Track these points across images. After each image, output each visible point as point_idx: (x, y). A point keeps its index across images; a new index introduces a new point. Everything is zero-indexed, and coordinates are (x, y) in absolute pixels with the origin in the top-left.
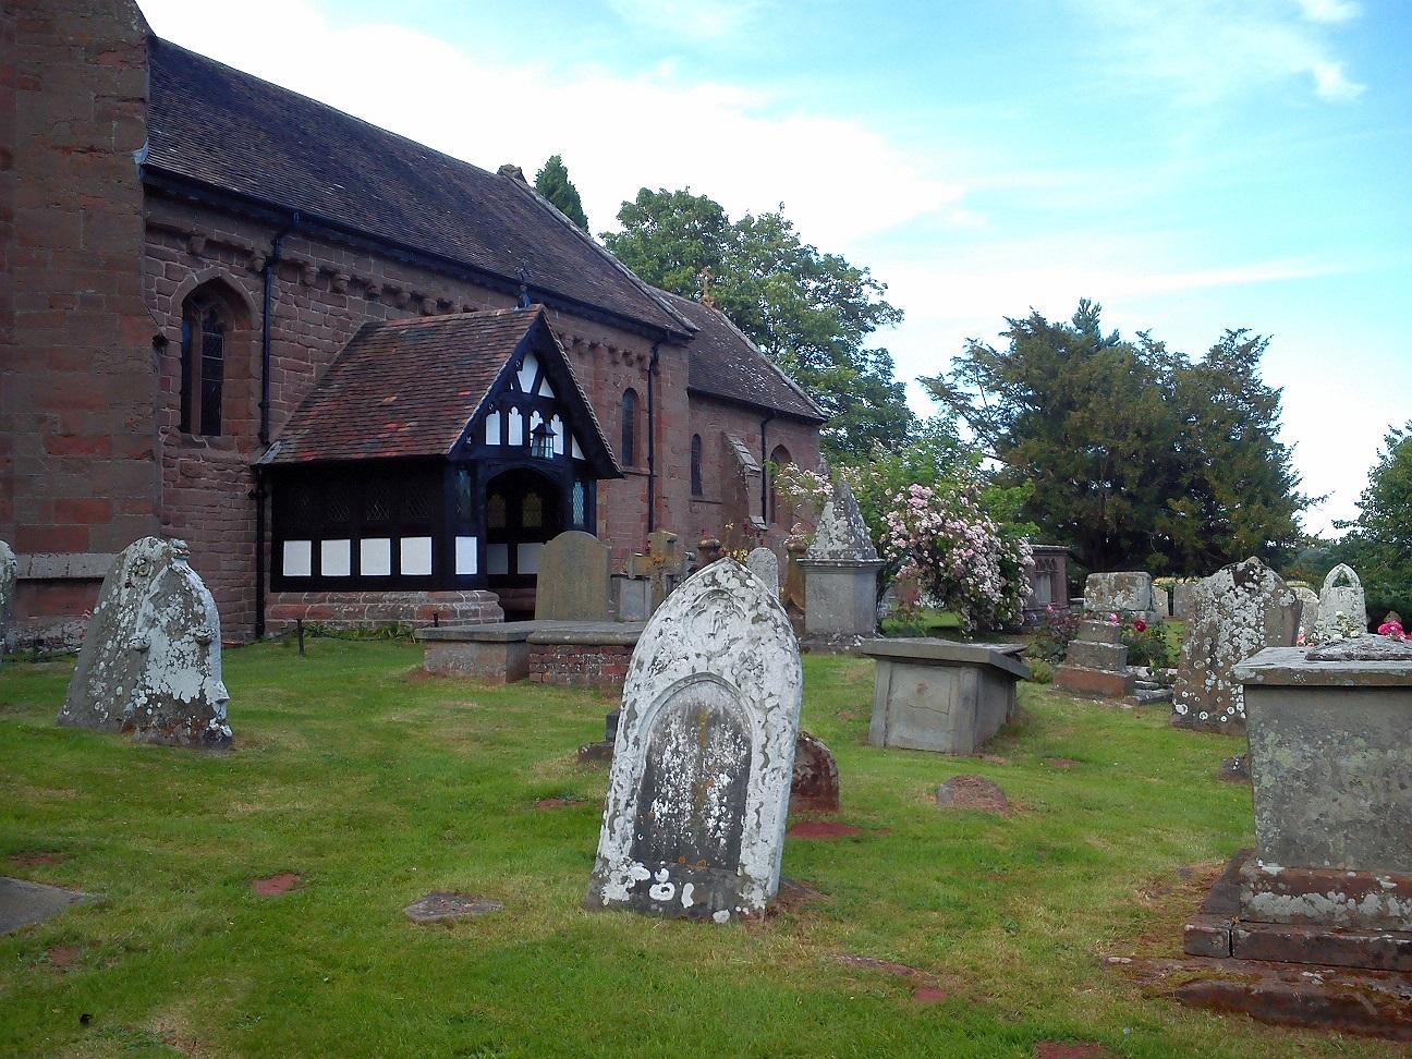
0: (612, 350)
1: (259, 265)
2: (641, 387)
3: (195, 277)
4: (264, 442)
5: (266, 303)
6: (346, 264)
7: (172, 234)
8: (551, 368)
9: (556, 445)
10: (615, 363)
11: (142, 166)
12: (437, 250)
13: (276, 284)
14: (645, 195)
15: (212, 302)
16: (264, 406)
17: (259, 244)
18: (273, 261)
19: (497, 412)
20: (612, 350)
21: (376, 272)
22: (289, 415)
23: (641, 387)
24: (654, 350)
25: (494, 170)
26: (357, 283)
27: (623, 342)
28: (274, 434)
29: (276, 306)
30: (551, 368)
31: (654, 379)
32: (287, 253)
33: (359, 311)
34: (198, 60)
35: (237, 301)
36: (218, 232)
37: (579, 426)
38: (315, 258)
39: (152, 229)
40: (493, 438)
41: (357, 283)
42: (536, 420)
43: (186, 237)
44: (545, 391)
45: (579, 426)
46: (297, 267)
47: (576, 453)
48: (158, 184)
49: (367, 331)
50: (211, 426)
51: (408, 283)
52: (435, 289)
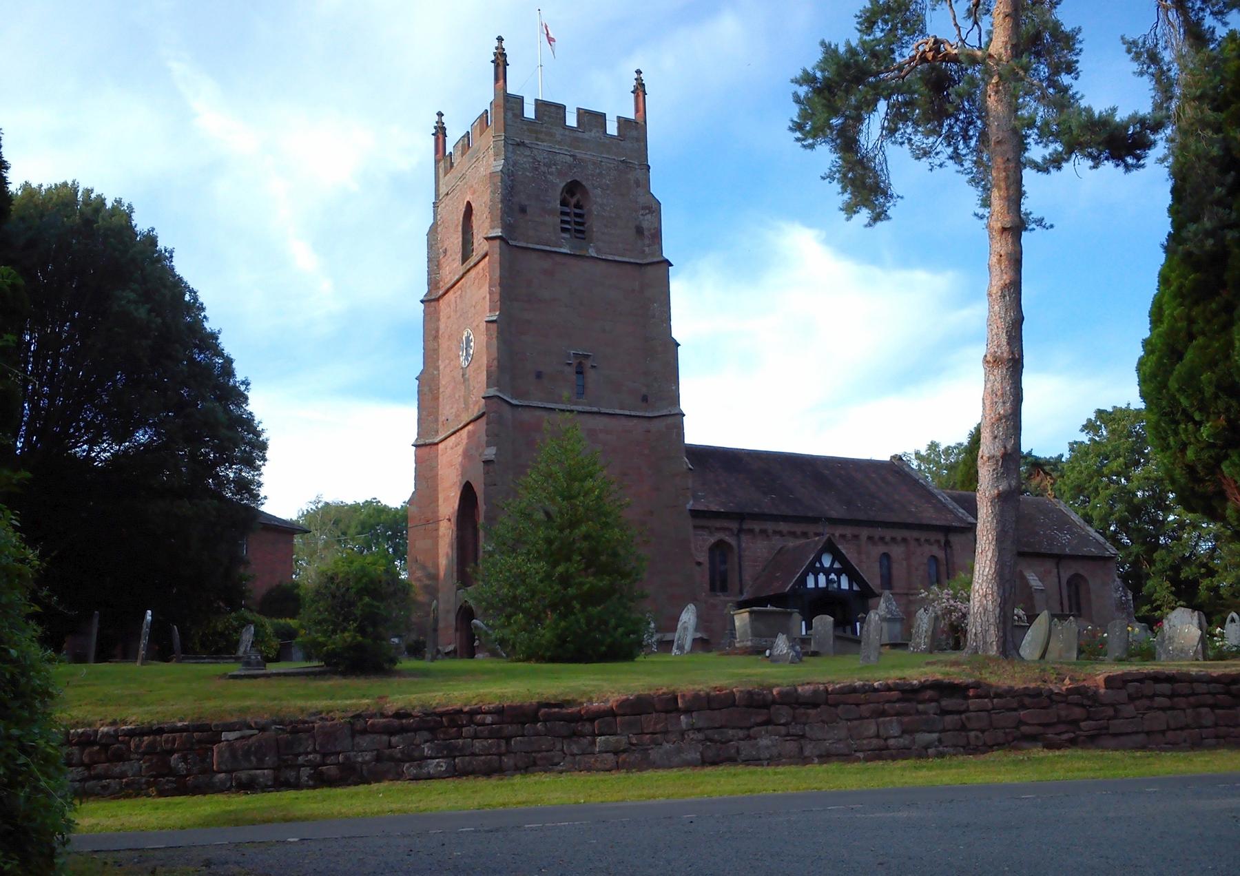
0: (917, 540)
1: (736, 532)
2: (941, 554)
3: (712, 540)
4: (741, 592)
5: (739, 546)
6: (770, 526)
7: (703, 528)
8: (837, 556)
9: (845, 584)
10: (920, 545)
11: (690, 510)
12: (810, 514)
13: (744, 537)
14: (1100, 413)
15: (720, 550)
16: (741, 581)
17: (734, 526)
18: (740, 531)
19: (810, 574)
20: (917, 540)
21: (783, 527)
22: (751, 583)
23: (941, 554)
24: (946, 536)
25: (888, 459)
26: (775, 532)
27: (923, 536)
28: (745, 590)
29: (744, 545)
30: (837, 556)
31: (948, 551)
32: (745, 526)
33: (777, 542)
34: (733, 452)
35: (729, 546)
36: (718, 524)
37: (854, 576)
38: (757, 526)
39: (695, 527)
40: (811, 583)
41: (775, 532)
42: (833, 576)
43: (708, 528)
44: (836, 565)
45: (854, 576)
46: (751, 531)
47: (855, 588)
48: (695, 514)
49: (782, 548)
50: (724, 588)
51: (799, 528)
52: (811, 529)
